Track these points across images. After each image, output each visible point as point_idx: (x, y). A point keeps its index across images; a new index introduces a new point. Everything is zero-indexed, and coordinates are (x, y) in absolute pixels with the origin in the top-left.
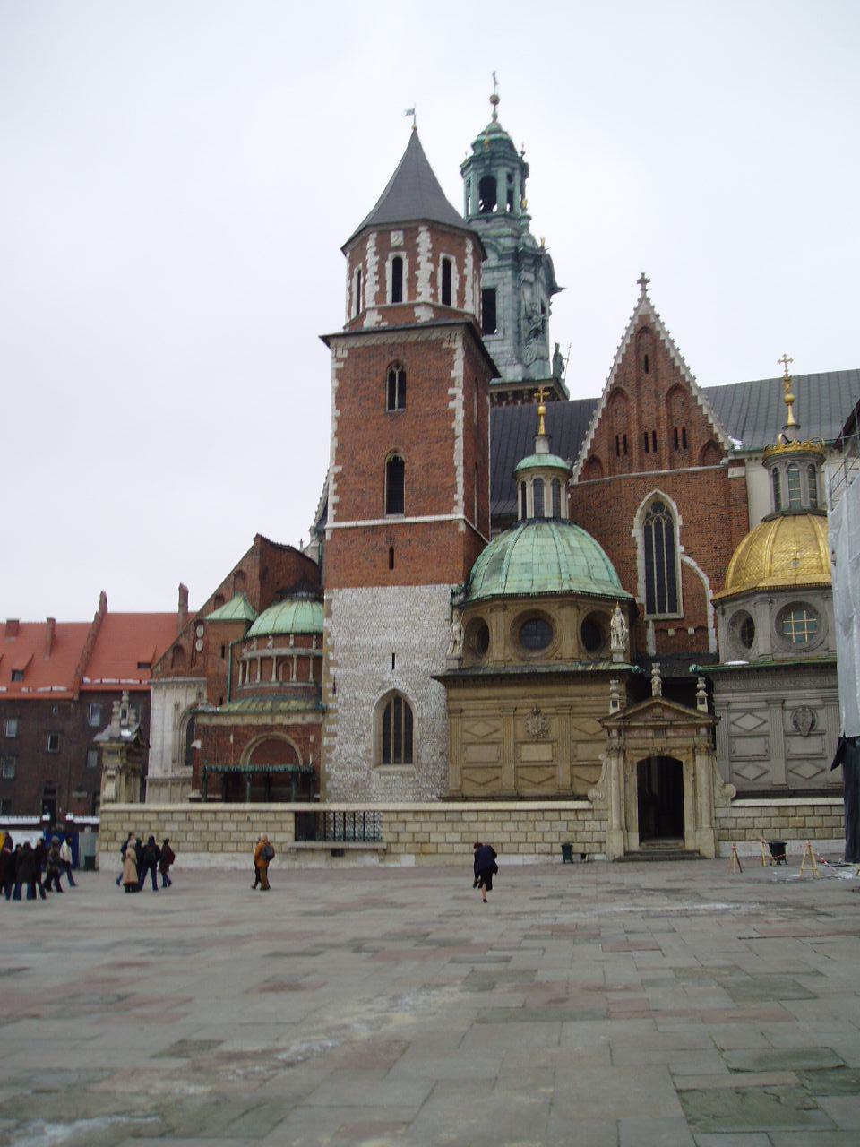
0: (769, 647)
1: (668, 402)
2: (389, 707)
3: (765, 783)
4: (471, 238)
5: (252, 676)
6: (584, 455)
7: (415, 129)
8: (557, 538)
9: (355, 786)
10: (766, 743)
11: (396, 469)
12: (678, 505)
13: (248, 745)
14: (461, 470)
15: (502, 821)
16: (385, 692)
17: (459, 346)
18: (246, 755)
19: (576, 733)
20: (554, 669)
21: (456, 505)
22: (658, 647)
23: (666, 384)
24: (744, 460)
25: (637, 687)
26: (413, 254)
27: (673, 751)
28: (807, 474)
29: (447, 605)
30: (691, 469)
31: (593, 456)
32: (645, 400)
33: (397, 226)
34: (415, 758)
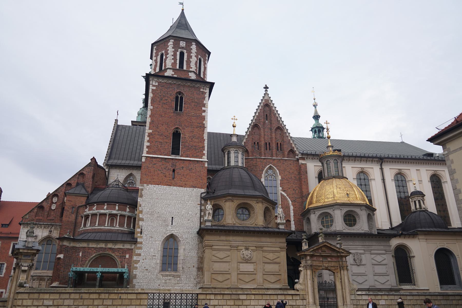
1: (275, 133)
5: (93, 224)
7: (183, 10)
11: (176, 136)
12: (279, 171)
16: (168, 235)
23: (275, 126)
24: (304, 158)
26: (189, 52)
32: (266, 130)
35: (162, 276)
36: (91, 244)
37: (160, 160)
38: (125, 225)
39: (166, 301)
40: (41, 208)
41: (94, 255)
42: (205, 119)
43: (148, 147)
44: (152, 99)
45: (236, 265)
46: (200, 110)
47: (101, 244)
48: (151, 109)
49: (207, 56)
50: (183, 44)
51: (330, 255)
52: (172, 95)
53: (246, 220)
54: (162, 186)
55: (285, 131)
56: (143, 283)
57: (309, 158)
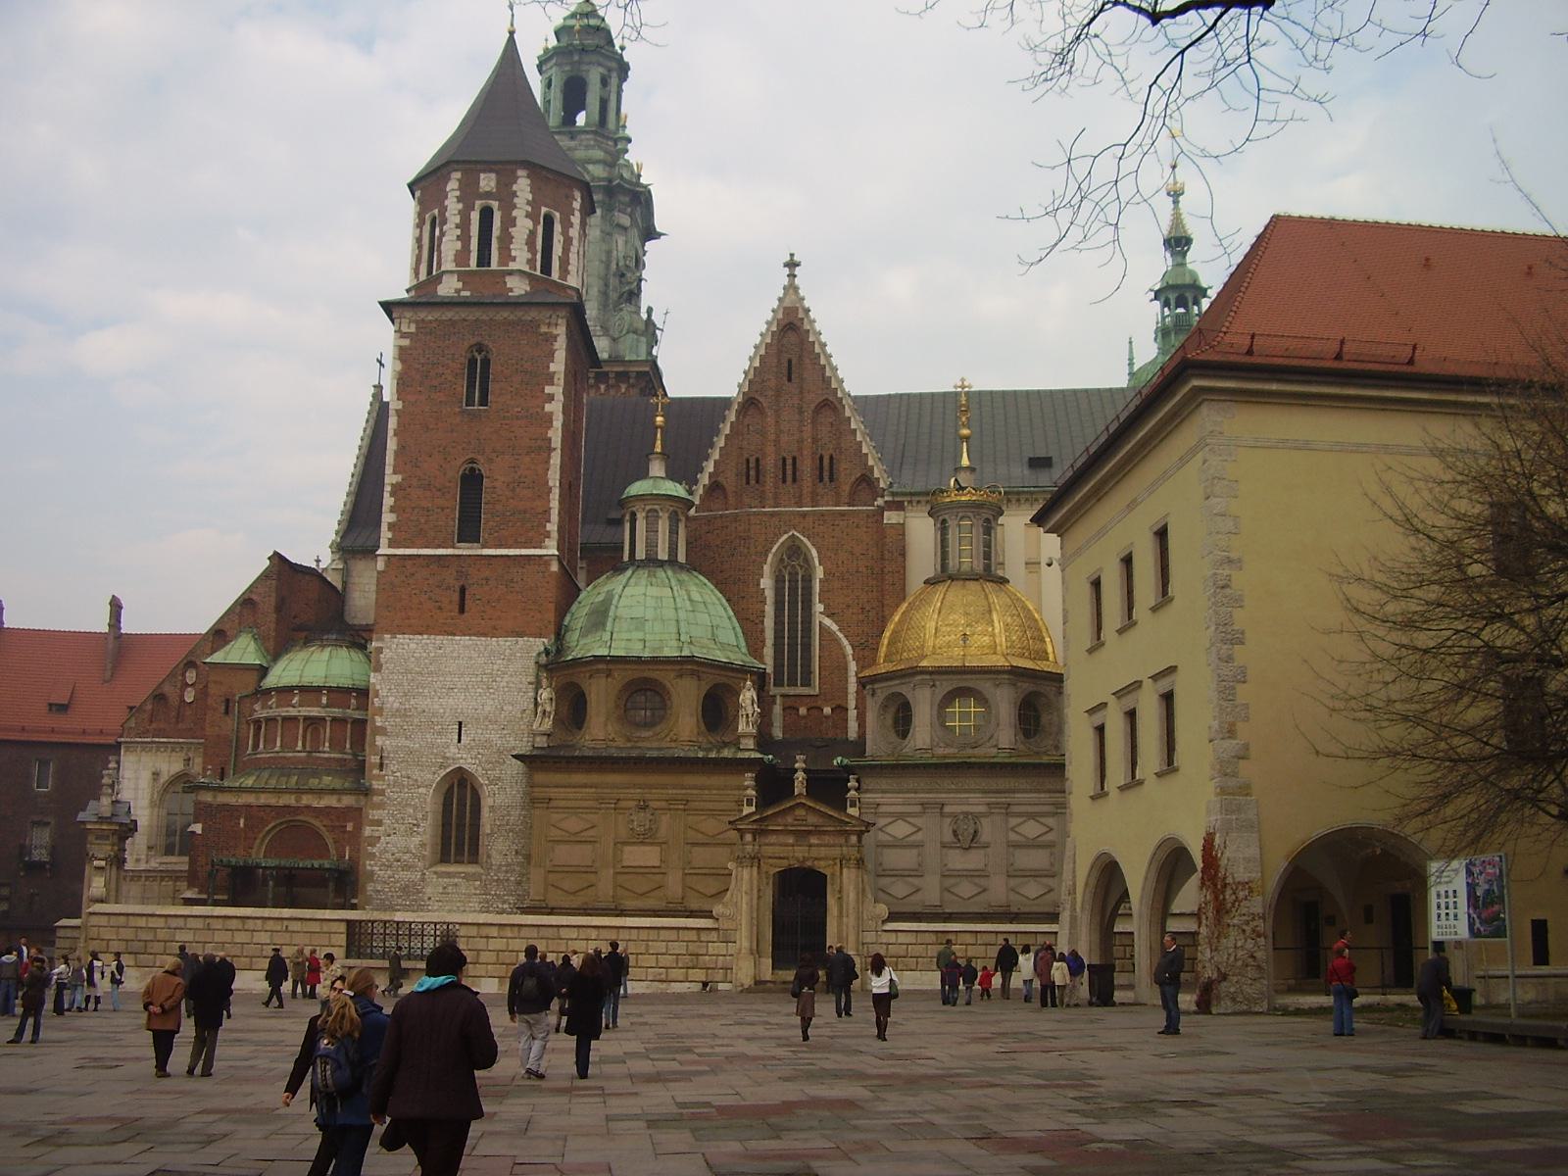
0: (928, 741)
1: (814, 422)
2: (451, 787)
3: (914, 905)
5: (270, 741)
6: (704, 479)
7: (512, 33)
8: (675, 588)
9: (405, 889)
10: (919, 855)
11: (472, 481)
13: (264, 833)
14: (556, 492)
16: (448, 770)
17: (561, 331)
18: (261, 844)
19: (691, 833)
20: (668, 754)
22: (785, 729)
23: (813, 399)
24: (903, 502)
25: (773, 786)
26: (508, 206)
27: (816, 862)
28: (981, 530)
29: (532, 664)
30: (838, 508)
31: (715, 482)
34: (483, 857)
35: (435, 876)
40: (161, 699)
41: (273, 824)
43: (391, 526)
44: (398, 379)
46: (539, 394)
48: (397, 411)
49: (578, 195)
50: (487, 182)
51: (813, 828)
52: (456, 356)
54: (433, 637)
56: (390, 894)
57: (919, 502)
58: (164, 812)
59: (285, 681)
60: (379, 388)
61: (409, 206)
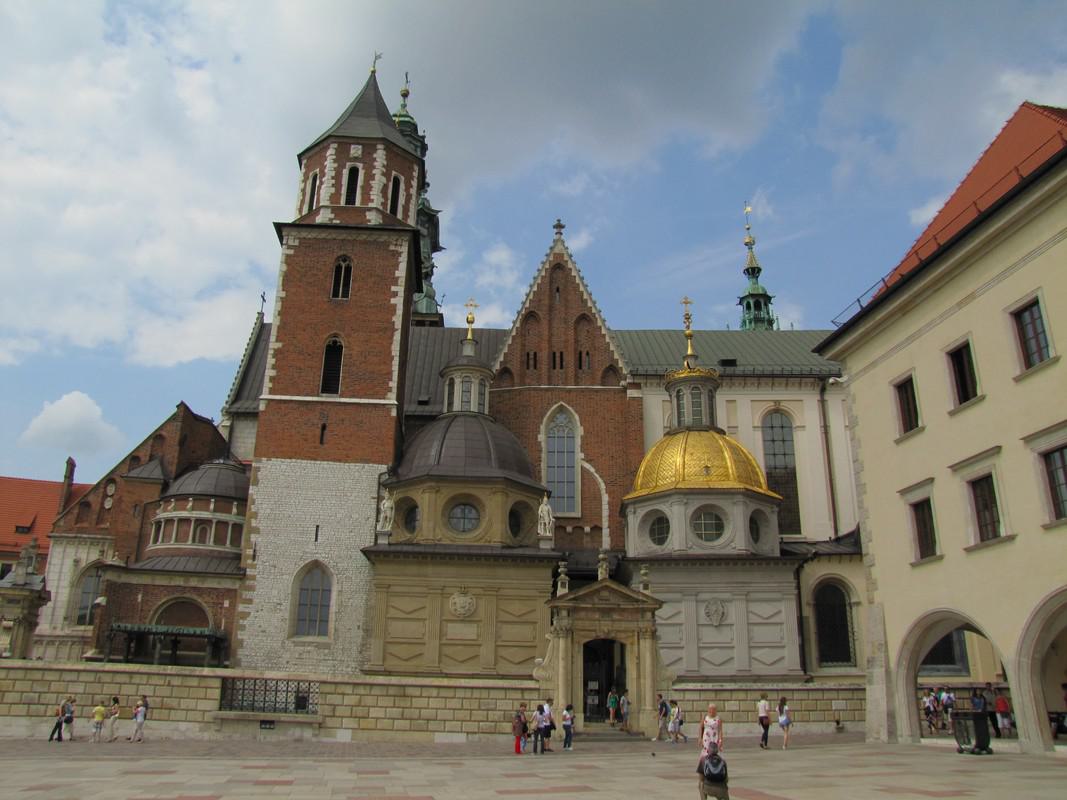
1: (575, 329)
4: (419, 165)
7: (373, 72)
11: (334, 351)
13: (156, 606)
15: (446, 698)
17: (404, 249)
21: (390, 391)
23: (575, 313)
24: (640, 384)
26: (369, 167)
33: (357, 140)
36: (158, 577)
37: (296, 406)
38: (228, 542)
39: (300, 695)
42: (395, 310)
43: (272, 379)
45: (438, 626)
47: (177, 578)
49: (416, 168)
51: (616, 606)
53: (470, 530)
55: (599, 323)
57: (651, 384)
58: (80, 591)
59: (184, 490)
60: (261, 315)
61: (297, 173)
